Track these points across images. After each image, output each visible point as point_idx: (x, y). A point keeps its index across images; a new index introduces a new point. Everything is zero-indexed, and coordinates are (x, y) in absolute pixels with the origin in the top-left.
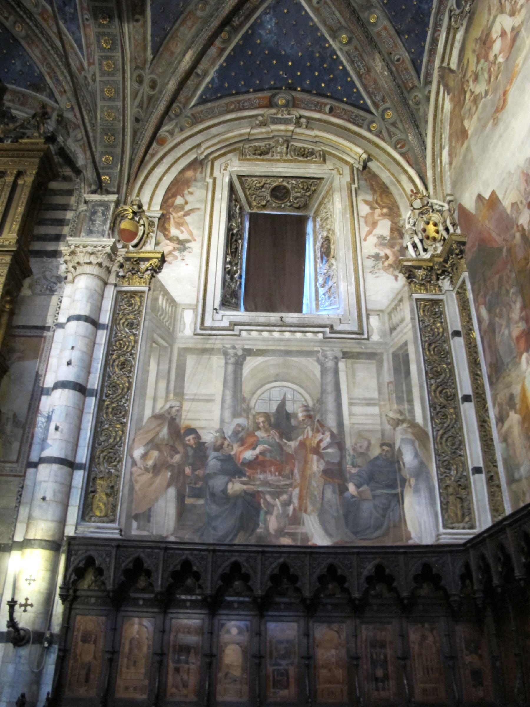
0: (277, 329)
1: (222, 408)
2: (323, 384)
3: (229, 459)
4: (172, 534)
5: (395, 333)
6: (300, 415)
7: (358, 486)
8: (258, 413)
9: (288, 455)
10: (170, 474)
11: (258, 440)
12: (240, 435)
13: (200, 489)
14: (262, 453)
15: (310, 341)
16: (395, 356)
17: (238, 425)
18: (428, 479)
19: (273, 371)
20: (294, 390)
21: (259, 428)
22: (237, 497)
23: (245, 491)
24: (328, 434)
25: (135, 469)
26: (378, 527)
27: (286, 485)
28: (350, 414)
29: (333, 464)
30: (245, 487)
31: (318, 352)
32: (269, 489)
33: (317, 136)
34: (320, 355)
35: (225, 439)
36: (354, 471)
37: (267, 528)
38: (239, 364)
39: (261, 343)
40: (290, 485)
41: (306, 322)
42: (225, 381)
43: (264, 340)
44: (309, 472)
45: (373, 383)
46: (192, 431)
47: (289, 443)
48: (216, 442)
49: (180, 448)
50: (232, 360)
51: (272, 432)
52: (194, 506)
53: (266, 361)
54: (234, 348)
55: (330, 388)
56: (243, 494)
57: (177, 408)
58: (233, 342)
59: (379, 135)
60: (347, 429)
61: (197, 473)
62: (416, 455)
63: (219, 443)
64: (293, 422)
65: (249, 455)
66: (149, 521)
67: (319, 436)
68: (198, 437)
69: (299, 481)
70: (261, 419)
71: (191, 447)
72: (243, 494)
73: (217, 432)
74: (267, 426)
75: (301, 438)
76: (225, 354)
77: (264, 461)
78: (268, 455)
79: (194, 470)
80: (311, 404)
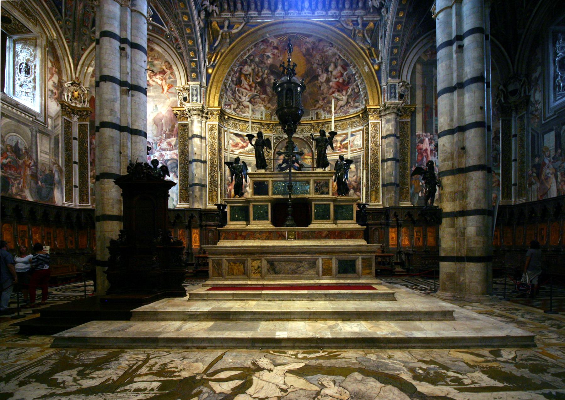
5: (56, 129)
6: (23, 150)
7: (42, 183)
16: (55, 138)
18: (61, 185)
21: (8, 151)
26: (47, 197)
28: (40, 156)
33: (37, 9)
34: (31, 127)
36: (41, 177)
37: (12, 191)
40: (20, 177)
44: (26, 174)
45: (48, 146)
51: (13, 154)
55: (34, 143)
59: (61, 28)
60: (39, 161)
62: (59, 177)
64: (21, 153)
67: (30, 161)
70: (9, 148)
80: (27, 147)
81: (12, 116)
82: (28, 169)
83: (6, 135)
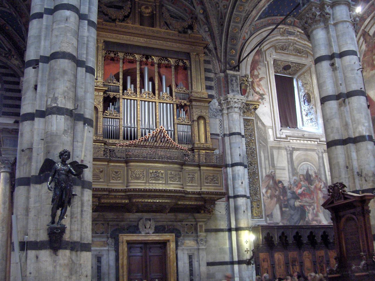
0: (302, 139)
1: (289, 173)
2: (319, 163)
3: (293, 193)
4: (281, 222)
8: (301, 175)
9: (312, 191)
10: (276, 199)
11: (302, 186)
12: (296, 183)
13: (287, 204)
14: (304, 190)
15: (313, 145)
17: (295, 179)
19: (303, 157)
20: (310, 165)
21: (301, 181)
22: (298, 207)
23: (301, 205)
24: (323, 183)
25: (264, 197)
27: (312, 202)
29: (325, 194)
30: (300, 203)
31: (316, 149)
32: (308, 204)
34: (317, 151)
35: (291, 185)
38: (291, 154)
39: (297, 145)
41: (311, 137)
42: (288, 162)
43: (298, 144)
44: (318, 198)
46: (280, 182)
47: (311, 186)
48: (288, 186)
49: (277, 189)
50: (289, 152)
51: (306, 182)
52: (285, 211)
53: (300, 153)
54: (289, 147)
55: (321, 165)
56: (300, 206)
57: (274, 172)
58: (288, 144)
61: (284, 198)
63: (290, 187)
64: (312, 178)
65: (300, 191)
66: (272, 217)
67: (320, 184)
68: (283, 184)
69: (316, 201)
70: (302, 177)
71: (281, 188)
72: (300, 206)
73: (288, 182)
74: (304, 180)
75: (315, 184)
76: (286, 149)
77: (305, 193)
78: (306, 191)
79: (283, 197)
80: (316, 171)
81: (301, 147)
82: (319, 192)
83: (298, 166)
